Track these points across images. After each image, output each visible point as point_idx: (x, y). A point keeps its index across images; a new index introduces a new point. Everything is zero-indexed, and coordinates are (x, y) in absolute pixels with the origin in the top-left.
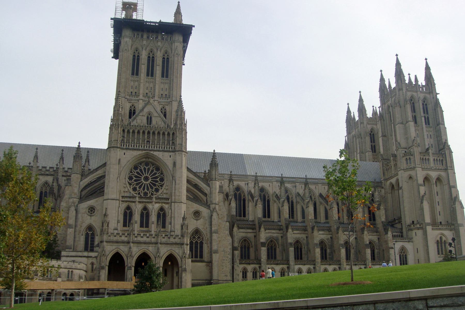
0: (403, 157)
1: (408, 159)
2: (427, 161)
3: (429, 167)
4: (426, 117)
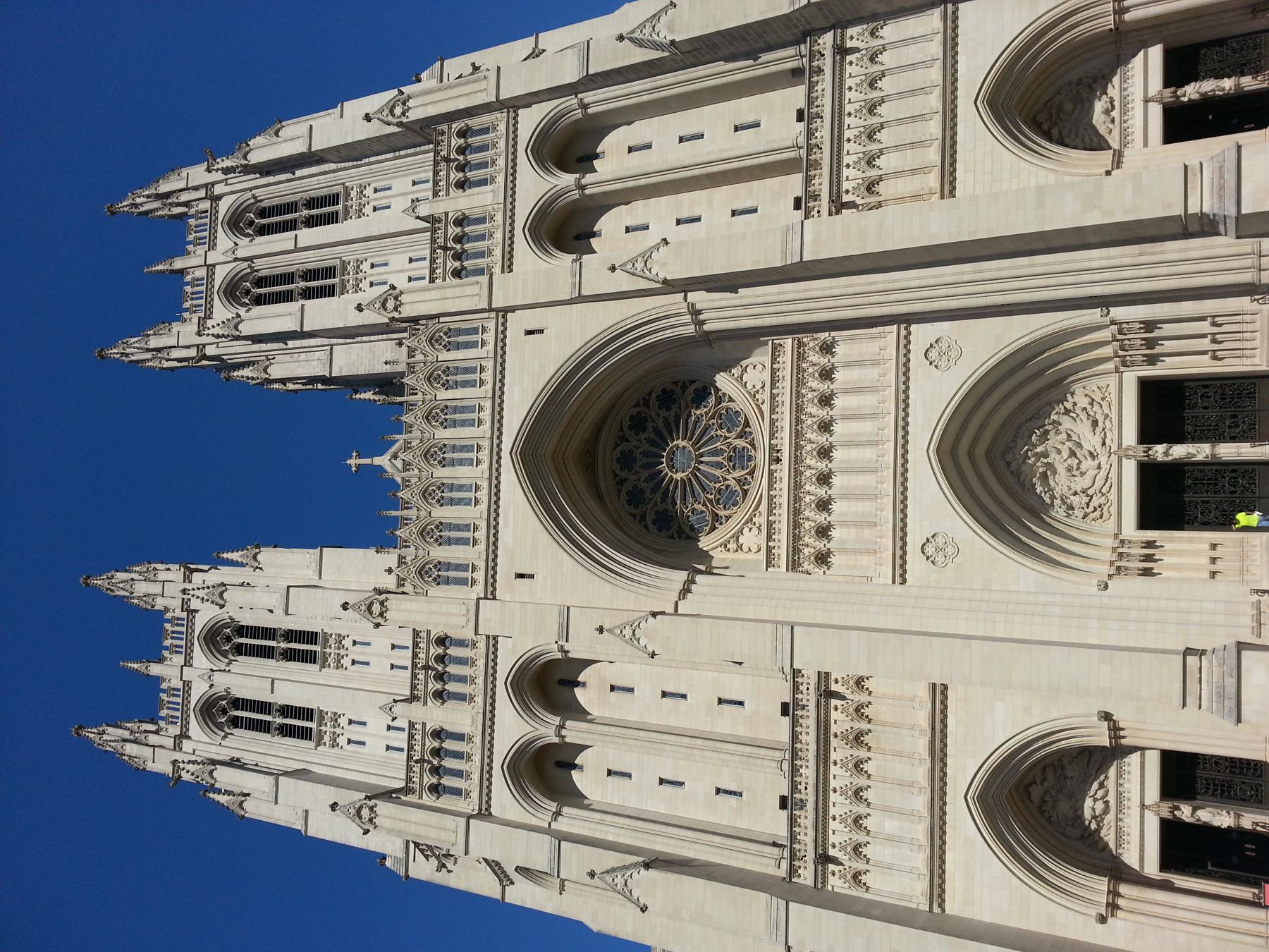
3: (499, 217)
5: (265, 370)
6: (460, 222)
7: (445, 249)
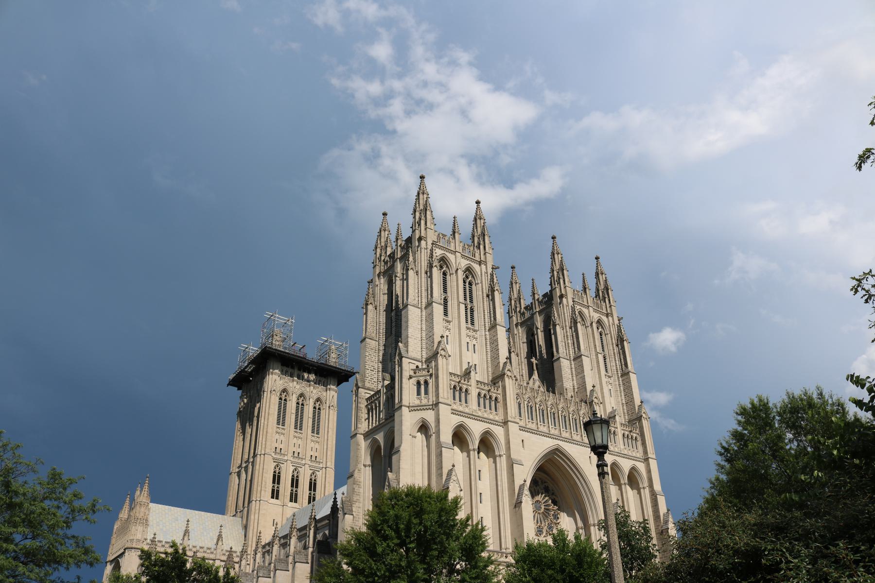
0: (411, 377)
1: (422, 382)
2: (463, 395)
3: (467, 410)
4: (469, 307)
5: (412, 269)
6: (466, 391)
7: (459, 382)
